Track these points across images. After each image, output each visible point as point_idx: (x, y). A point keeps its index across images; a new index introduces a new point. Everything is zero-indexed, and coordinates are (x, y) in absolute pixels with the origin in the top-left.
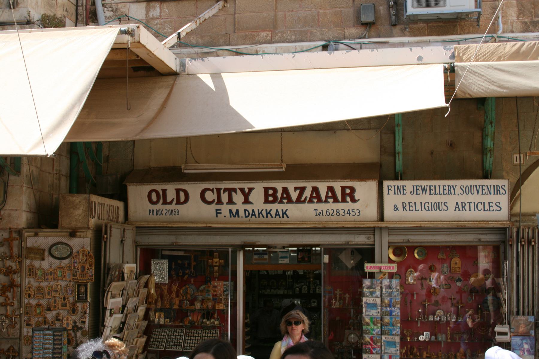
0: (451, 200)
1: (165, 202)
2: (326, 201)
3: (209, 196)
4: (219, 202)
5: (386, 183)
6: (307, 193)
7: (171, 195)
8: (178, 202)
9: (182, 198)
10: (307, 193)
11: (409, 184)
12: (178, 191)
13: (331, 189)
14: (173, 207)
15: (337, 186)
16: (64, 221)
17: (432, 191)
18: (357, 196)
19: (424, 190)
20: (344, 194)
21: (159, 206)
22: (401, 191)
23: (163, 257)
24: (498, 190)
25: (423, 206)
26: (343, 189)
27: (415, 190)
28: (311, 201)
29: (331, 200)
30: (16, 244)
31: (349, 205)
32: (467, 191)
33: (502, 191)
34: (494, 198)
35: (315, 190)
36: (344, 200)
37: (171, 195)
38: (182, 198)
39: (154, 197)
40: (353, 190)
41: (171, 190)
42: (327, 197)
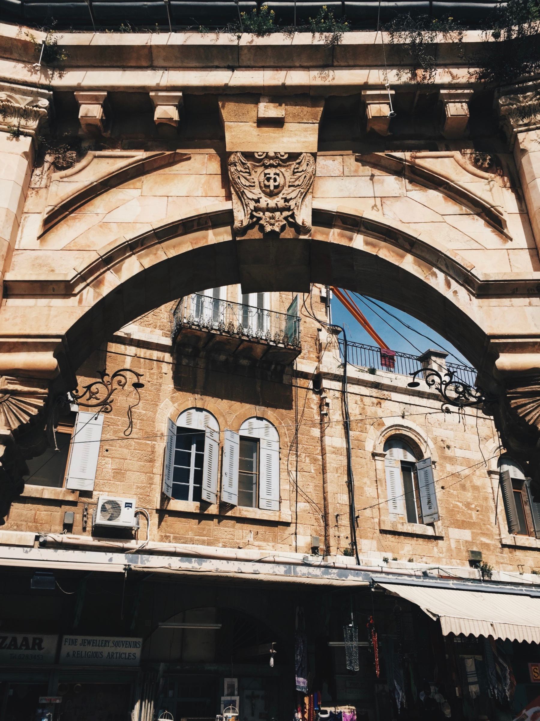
2: (20, 648)
5: (65, 637)
6: (8, 641)
10: (8, 641)
11: (80, 638)
13: (25, 639)
15: (31, 637)
18: (43, 645)
19: (89, 643)
20: (34, 643)
22: (74, 642)
24: (135, 645)
26: (35, 639)
27: (83, 643)
28: (9, 648)
29: (24, 648)
33: (138, 646)
35: (14, 639)
36: (33, 648)
40: (41, 640)
42: (22, 645)
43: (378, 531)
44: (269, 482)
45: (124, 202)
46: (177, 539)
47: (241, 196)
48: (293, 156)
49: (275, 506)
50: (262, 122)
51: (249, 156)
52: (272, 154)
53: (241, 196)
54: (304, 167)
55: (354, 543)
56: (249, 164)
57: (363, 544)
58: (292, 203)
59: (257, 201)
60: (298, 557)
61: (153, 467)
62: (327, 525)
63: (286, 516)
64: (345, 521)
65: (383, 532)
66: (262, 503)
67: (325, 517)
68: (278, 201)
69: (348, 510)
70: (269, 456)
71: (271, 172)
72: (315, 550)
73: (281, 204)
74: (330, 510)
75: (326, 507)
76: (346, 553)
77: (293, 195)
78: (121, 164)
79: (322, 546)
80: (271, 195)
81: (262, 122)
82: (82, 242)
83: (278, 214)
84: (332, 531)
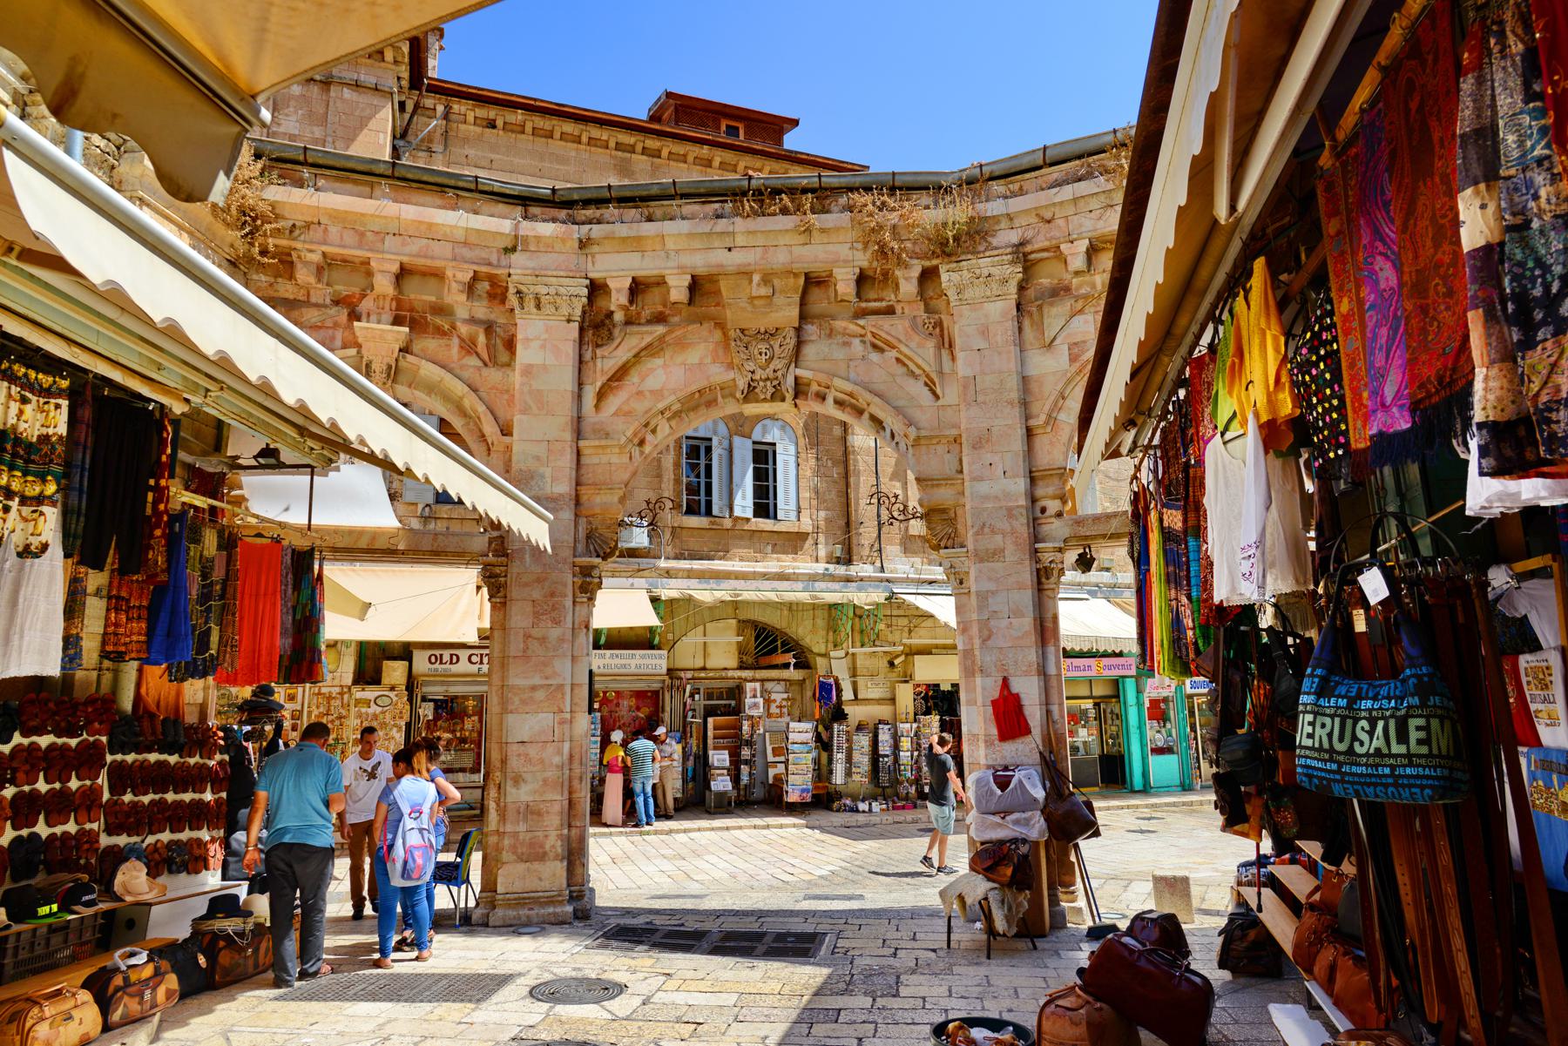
0: (633, 662)
1: (441, 663)
3: (474, 659)
4: (481, 663)
7: (446, 658)
8: (451, 663)
9: (455, 658)
11: (608, 652)
12: (451, 655)
14: (448, 666)
16: (386, 680)
17: (621, 657)
21: (437, 665)
22: (603, 656)
23: (430, 700)
25: (616, 666)
30: (346, 697)
32: (643, 657)
34: (658, 662)
37: (446, 658)
38: (455, 658)
39: (433, 659)
41: (446, 654)
44: (786, 492)
45: (653, 370)
46: (692, 557)
49: (793, 516)
52: (762, 330)
54: (788, 340)
56: (746, 339)
58: (779, 374)
59: (753, 372)
60: (820, 568)
61: (660, 482)
63: (806, 524)
66: (780, 515)
68: (769, 372)
70: (786, 462)
73: (771, 375)
77: (779, 366)
82: (626, 408)
83: (768, 383)
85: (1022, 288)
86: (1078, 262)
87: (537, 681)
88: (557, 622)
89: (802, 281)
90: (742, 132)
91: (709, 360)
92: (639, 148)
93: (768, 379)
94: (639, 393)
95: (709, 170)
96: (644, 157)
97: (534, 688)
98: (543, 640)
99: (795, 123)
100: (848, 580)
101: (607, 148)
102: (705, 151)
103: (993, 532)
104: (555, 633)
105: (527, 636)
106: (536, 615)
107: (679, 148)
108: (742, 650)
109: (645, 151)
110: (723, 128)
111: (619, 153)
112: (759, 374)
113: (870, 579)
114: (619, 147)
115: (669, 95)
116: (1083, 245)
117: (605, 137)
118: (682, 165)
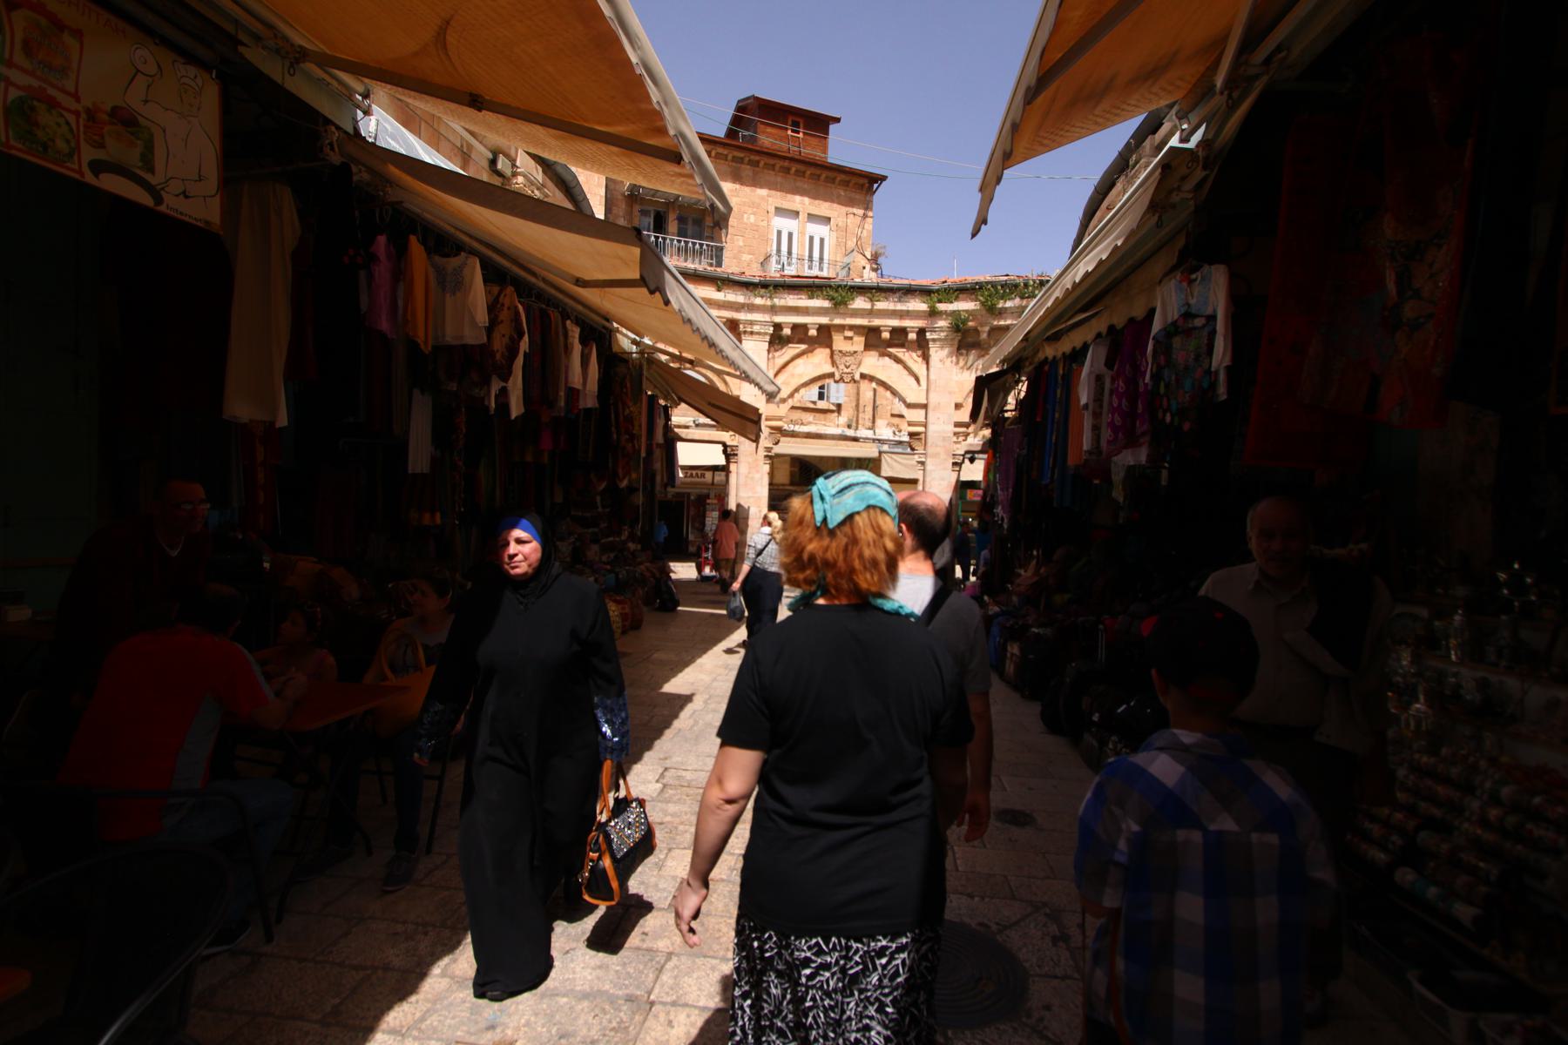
10: (688, 475)
31: (702, 479)
43: (889, 415)
47: (837, 367)
48: (855, 352)
50: (847, 338)
51: (840, 351)
53: (837, 367)
55: (874, 422)
57: (879, 422)
60: (838, 431)
62: (858, 411)
64: (869, 409)
65: (893, 415)
67: (857, 406)
68: (849, 370)
69: (872, 401)
71: (848, 358)
72: (849, 427)
74: (861, 402)
75: (858, 400)
76: (869, 429)
78: (797, 351)
79: (854, 424)
80: (847, 367)
81: (847, 338)
84: (861, 415)
85: (960, 341)
86: (984, 336)
87: (750, 494)
88: (758, 472)
89: (866, 330)
90: (801, 125)
91: (823, 362)
92: (747, 159)
93: (848, 374)
94: (793, 375)
95: (788, 176)
96: (749, 167)
97: (749, 497)
98: (752, 478)
99: (837, 120)
100: (855, 439)
101: (726, 160)
102: (786, 164)
103: (937, 446)
104: (757, 476)
105: (746, 477)
106: (750, 468)
107: (772, 161)
108: (792, 475)
109: (751, 163)
110: (790, 122)
111: (734, 164)
112: (846, 370)
113: (866, 439)
114: (735, 159)
115: (757, 99)
116: (987, 329)
117: (725, 152)
118: (771, 172)
